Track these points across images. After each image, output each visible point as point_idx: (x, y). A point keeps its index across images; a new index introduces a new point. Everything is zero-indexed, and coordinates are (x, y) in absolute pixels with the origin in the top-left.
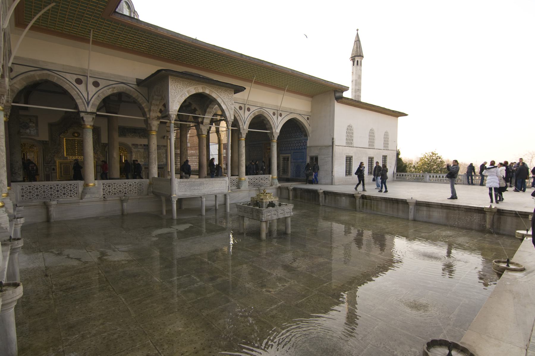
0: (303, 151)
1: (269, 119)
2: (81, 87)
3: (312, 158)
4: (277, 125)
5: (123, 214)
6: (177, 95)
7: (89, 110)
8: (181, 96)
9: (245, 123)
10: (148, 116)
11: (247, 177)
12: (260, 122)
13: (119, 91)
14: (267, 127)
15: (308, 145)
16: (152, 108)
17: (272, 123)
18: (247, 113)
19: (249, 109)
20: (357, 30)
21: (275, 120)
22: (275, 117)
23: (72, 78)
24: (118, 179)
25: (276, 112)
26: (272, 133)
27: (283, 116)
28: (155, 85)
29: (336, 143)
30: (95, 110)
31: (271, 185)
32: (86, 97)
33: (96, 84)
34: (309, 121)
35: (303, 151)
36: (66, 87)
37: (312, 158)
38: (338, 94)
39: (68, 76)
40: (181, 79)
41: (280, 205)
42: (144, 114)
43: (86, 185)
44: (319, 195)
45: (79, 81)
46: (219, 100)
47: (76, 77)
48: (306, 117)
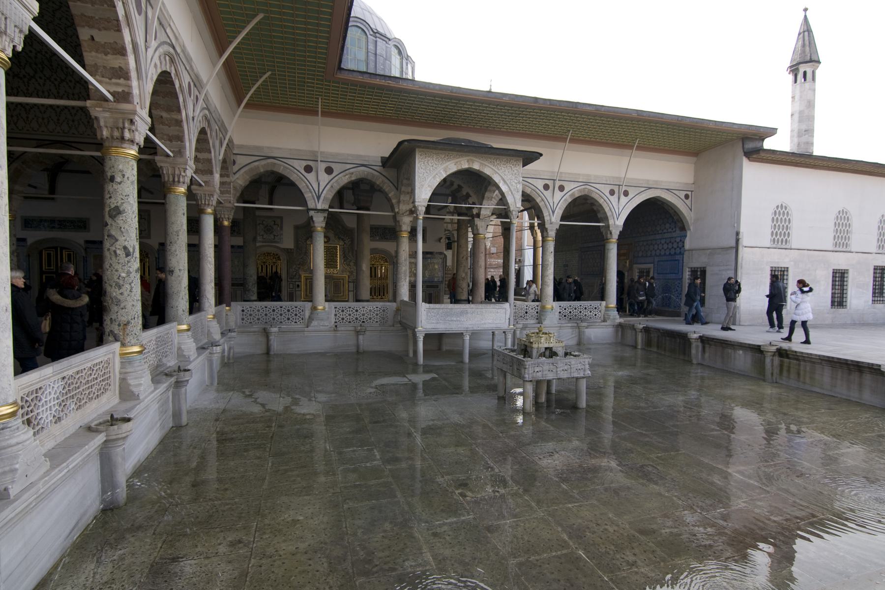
0: (677, 257)
1: (601, 201)
2: (311, 177)
3: (694, 272)
4: (618, 212)
5: (358, 352)
6: (429, 176)
7: (319, 207)
8: (434, 177)
9: (553, 212)
10: (397, 210)
11: (556, 304)
12: (585, 208)
13: (359, 177)
14: (599, 216)
15: (687, 246)
16: (402, 198)
17: (607, 209)
18: (558, 194)
19: (561, 188)
20: (806, 10)
21: (615, 203)
22: (614, 199)
23: (300, 165)
24: (368, 301)
25: (616, 189)
26: (608, 227)
27: (630, 196)
28: (400, 162)
29: (745, 240)
30: (327, 207)
31: (604, 321)
32: (316, 190)
33: (329, 171)
34: (688, 202)
35: (677, 257)
36: (293, 178)
37: (694, 272)
38: (750, 145)
39: (296, 164)
40: (434, 151)
41: (566, 354)
42: (393, 209)
43: (314, 308)
44: (690, 344)
45: (308, 169)
46: (496, 178)
47: (305, 163)
48: (682, 196)
